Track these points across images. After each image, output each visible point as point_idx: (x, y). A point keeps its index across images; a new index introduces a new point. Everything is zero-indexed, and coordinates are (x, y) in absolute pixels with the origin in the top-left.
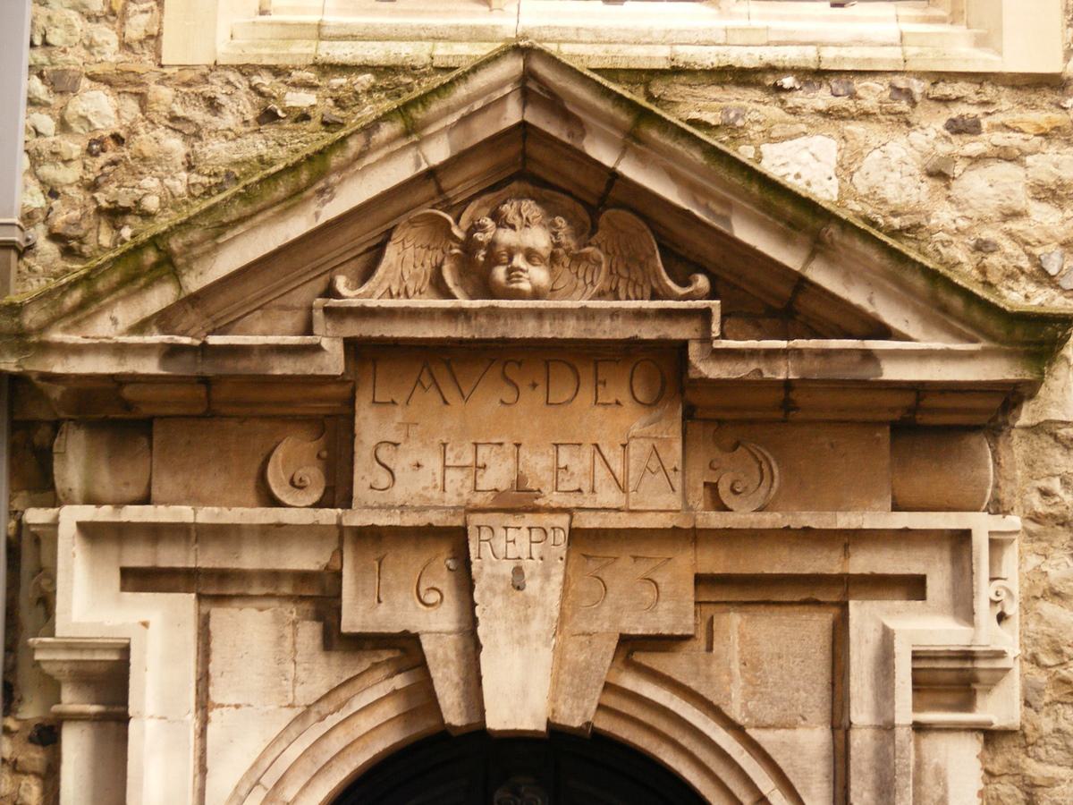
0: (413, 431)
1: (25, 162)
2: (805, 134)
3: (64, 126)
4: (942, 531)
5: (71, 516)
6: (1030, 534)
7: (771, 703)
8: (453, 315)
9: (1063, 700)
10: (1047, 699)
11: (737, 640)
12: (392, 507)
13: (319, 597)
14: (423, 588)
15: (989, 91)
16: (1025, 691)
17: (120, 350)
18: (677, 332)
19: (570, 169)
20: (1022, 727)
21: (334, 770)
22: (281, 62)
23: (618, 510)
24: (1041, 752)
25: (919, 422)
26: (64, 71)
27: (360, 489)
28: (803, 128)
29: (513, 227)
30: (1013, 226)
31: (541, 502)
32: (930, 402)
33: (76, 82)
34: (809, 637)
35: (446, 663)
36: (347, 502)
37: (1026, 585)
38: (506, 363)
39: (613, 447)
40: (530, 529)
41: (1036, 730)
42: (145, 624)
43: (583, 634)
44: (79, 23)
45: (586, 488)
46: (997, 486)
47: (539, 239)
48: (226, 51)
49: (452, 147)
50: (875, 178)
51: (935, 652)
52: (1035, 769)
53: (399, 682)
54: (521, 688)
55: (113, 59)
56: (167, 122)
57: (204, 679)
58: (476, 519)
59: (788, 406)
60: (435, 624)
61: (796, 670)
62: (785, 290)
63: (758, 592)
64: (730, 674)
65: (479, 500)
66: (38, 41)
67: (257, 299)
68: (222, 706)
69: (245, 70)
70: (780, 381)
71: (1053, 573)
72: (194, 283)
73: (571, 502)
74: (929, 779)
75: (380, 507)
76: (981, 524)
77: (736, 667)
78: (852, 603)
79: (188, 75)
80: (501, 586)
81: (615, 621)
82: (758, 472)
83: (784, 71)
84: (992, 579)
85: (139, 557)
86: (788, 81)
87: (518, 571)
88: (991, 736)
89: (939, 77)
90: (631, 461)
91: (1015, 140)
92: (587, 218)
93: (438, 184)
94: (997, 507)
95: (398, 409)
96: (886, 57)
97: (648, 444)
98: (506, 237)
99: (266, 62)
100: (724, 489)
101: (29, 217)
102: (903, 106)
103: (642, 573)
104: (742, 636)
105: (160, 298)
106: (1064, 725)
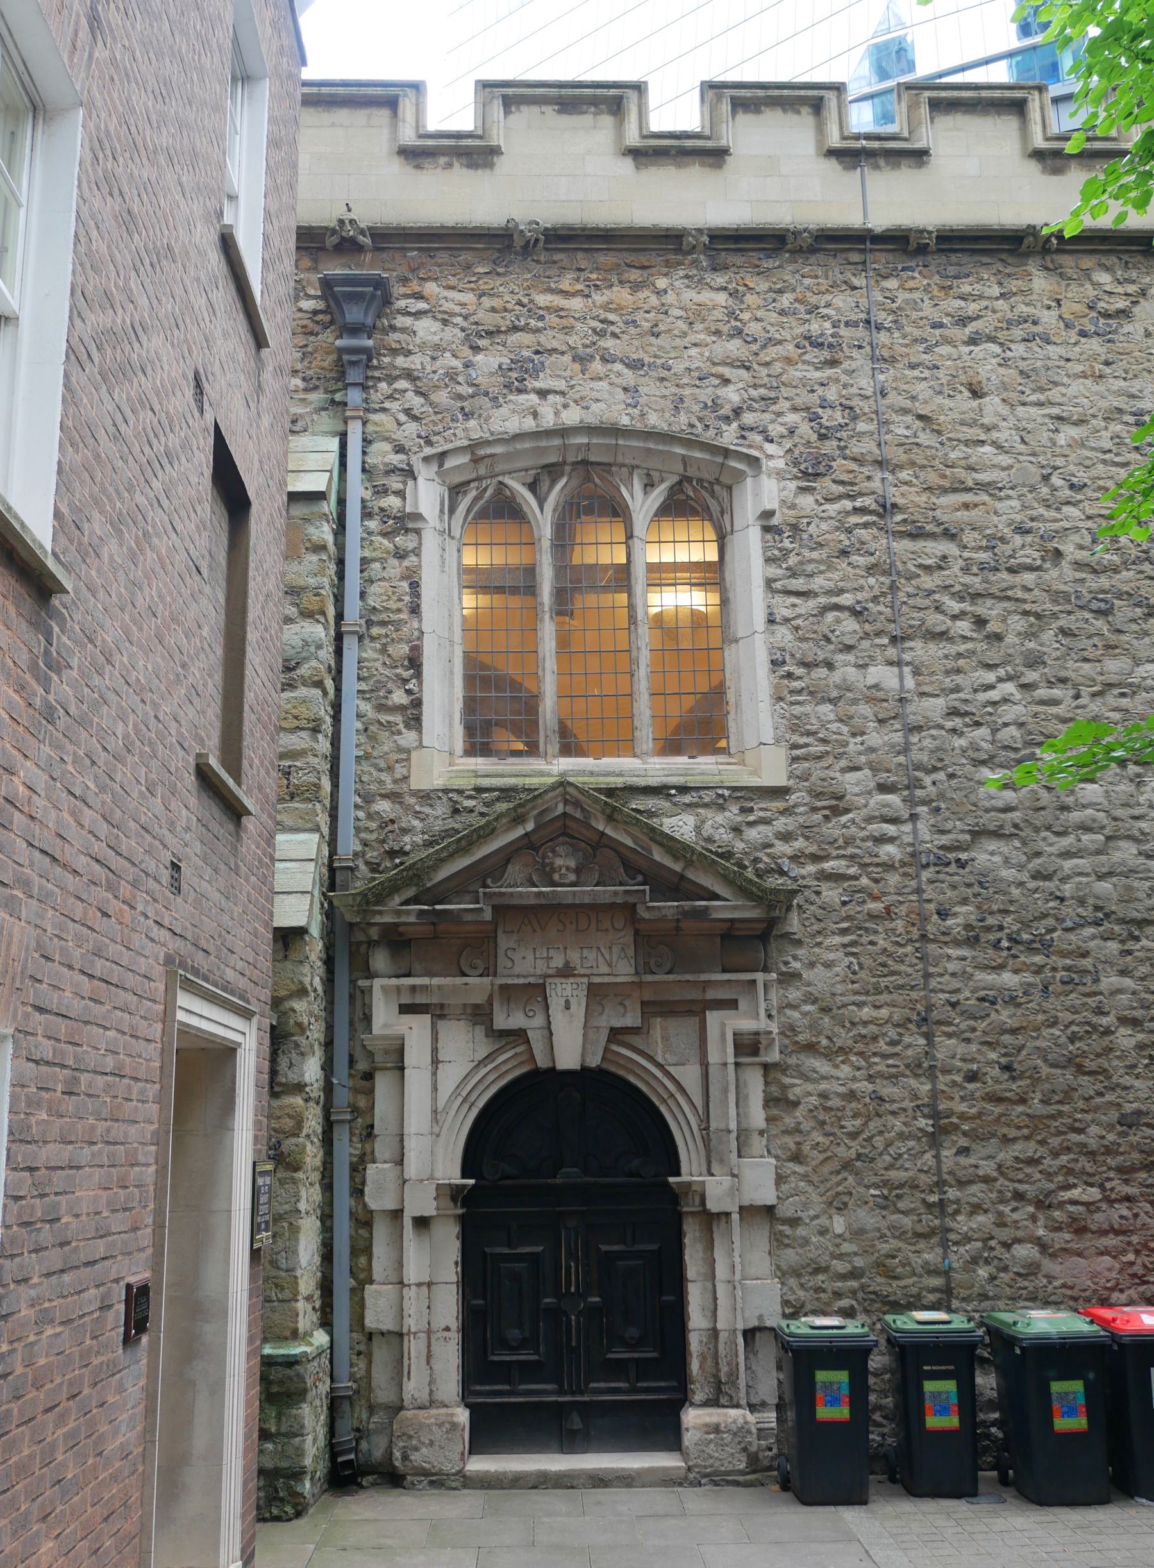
1: (353, 831)
3: (370, 816)
5: (377, 983)
8: (539, 894)
17: (398, 913)
18: (631, 900)
19: (584, 831)
32: (737, 925)
36: (495, 975)
44: (375, 773)
48: (439, 782)
50: (711, 831)
52: (787, 1081)
53: (519, 1049)
57: (435, 1050)
58: (549, 980)
59: (678, 929)
60: (533, 1024)
65: (550, 972)
69: (446, 791)
76: (760, 977)
85: (406, 1000)
86: (673, 792)
87: (567, 1003)
88: (766, 1067)
89: (734, 789)
91: (769, 814)
94: (766, 969)
96: (713, 781)
98: (559, 862)
100: (652, 963)
101: (356, 854)
102: (721, 801)
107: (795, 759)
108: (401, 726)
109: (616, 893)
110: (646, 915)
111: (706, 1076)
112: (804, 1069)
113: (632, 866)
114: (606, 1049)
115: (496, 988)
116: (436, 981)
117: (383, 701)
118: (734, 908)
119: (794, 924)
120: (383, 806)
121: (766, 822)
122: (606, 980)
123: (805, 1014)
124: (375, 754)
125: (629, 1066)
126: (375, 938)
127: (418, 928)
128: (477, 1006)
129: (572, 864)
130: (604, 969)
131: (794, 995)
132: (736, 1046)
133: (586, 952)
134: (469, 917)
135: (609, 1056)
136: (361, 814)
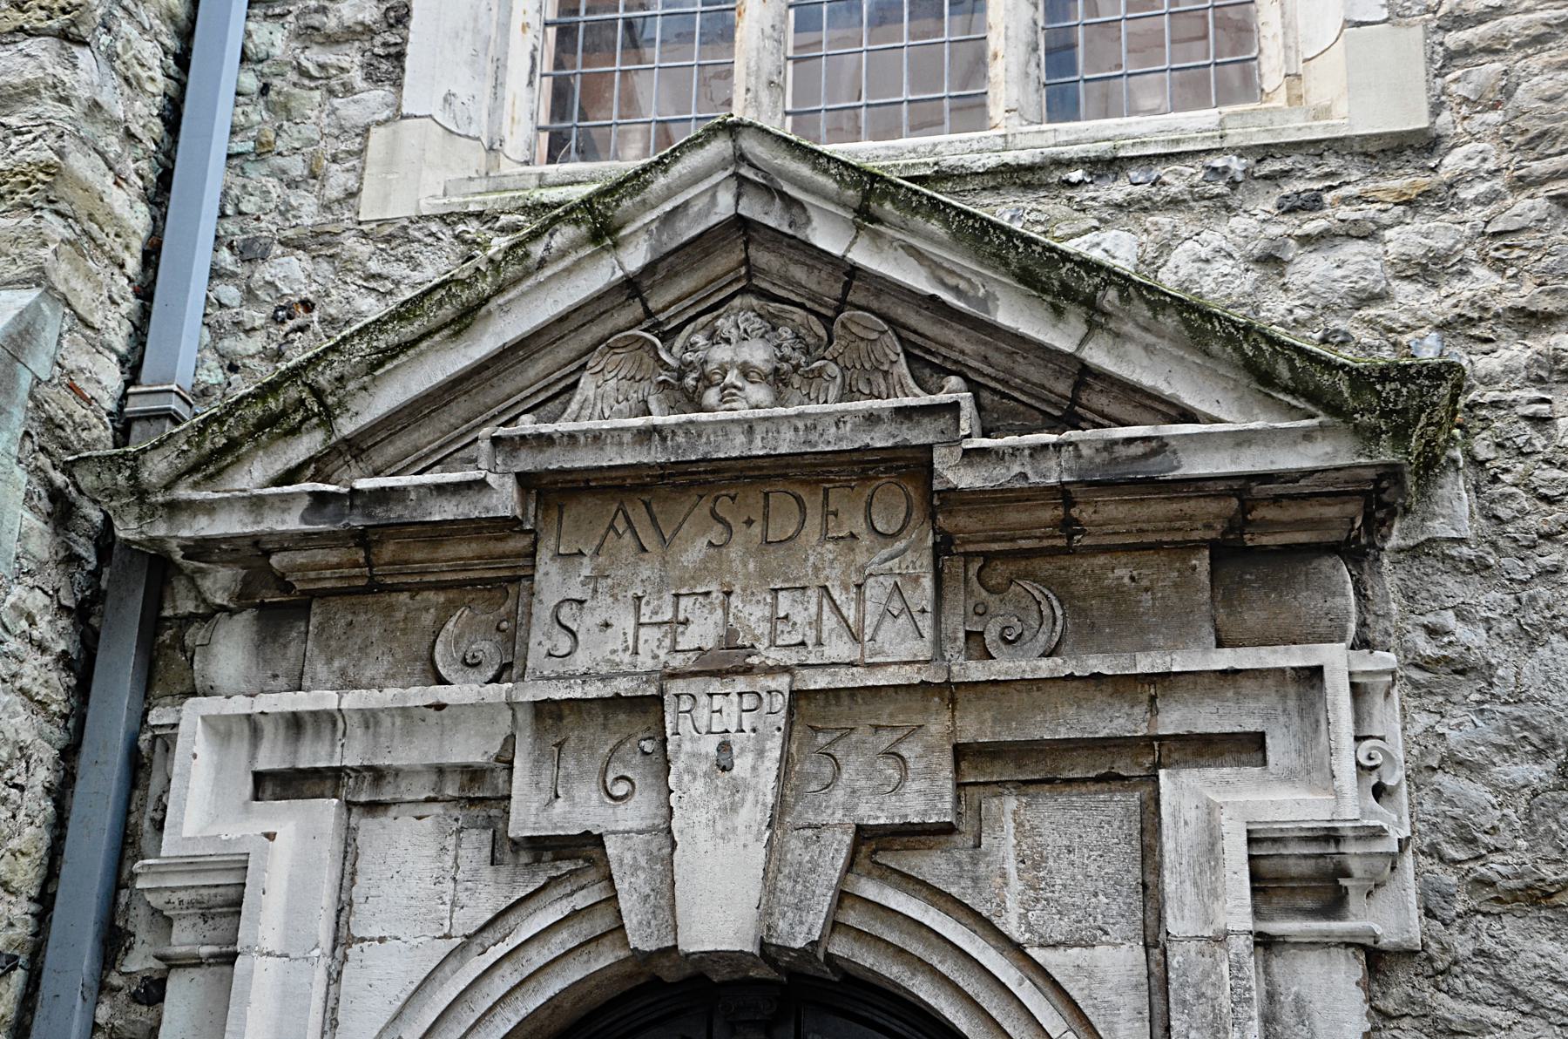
0: (603, 584)
2: (1097, 229)
3: (250, 295)
4: (1282, 670)
6: (1416, 685)
7: (1059, 912)
9: (1484, 908)
10: (1460, 908)
11: (1012, 831)
12: (573, 676)
13: (477, 793)
14: (610, 777)
15: (1333, 163)
16: (1423, 895)
17: (257, 504)
18: (917, 436)
20: (1425, 945)
21: (497, 1020)
22: (488, 209)
23: (852, 664)
24: (1459, 984)
25: (1250, 544)
26: (256, 239)
27: (536, 657)
28: (1096, 223)
29: (728, 341)
30: (1370, 312)
31: (754, 660)
33: (267, 249)
34: (1109, 823)
35: (636, 867)
37: (1415, 752)
38: (717, 498)
39: (846, 588)
40: (740, 694)
41: (1445, 950)
42: (270, 836)
43: (809, 826)
45: (810, 642)
46: (1363, 624)
47: (758, 354)
49: (653, 249)
51: (1281, 830)
54: (720, 892)
55: (308, 221)
56: (360, 282)
57: (343, 909)
58: (677, 686)
59: (1068, 526)
60: (622, 821)
61: (1092, 869)
62: (1063, 387)
63: (1040, 767)
64: (1004, 875)
65: (677, 662)
66: (229, 210)
67: (434, 451)
68: (363, 940)
70: (1052, 488)
71: (1453, 736)
72: (347, 426)
73: (790, 658)
74: (1287, 1016)
75: (558, 678)
76: (1335, 659)
77: (1011, 866)
78: (1162, 773)
79: (387, 230)
80: (704, 767)
81: (848, 810)
82: (1036, 615)
83: (1070, 164)
84: (1358, 739)
85: (271, 758)
86: (1076, 175)
88: (1377, 961)
90: (868, 604)
91: (1371, 210)
92: (822, 333)
93: (644, 304)
95: (586, 561)
97: (889, 582)
99: (471, 208)
100: (991, 636)
103: (883, 747)
104: (1019, 825)
105: (308, 444)
106: (1488, 944)
107: (1451, 56)
108: (357, 77)
109: (872, 419)
110: (967, 479)
111: (1158, 983)
112: (1514, 972)
113: (928, 339)
114: (843, 897)
115: (524, 717)
116: (352, 700)
117: (316, 20)
118: (1242, 439)
119: (1454, 510)
120: (291, 273)
121: (1370, 233)
122: (844, 679)
123: (1507, 792)
124: (280, 145)
125: (916, 948)
126: (220, 599)
127: (320, 556)
128: (473, 774)
129: (758, 354)
130: (839, 649)
131: (1462, 729)
132: (1263, 884)
133: (785, 603)
134: (445, 510)
135: (852, 918)
136: (229, 293)
